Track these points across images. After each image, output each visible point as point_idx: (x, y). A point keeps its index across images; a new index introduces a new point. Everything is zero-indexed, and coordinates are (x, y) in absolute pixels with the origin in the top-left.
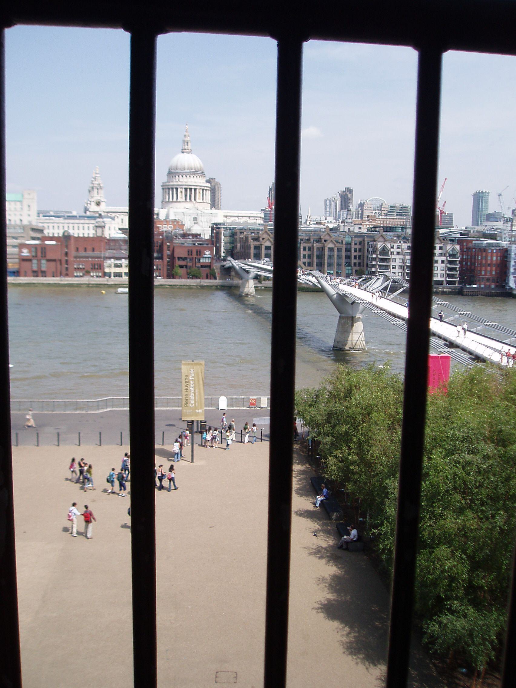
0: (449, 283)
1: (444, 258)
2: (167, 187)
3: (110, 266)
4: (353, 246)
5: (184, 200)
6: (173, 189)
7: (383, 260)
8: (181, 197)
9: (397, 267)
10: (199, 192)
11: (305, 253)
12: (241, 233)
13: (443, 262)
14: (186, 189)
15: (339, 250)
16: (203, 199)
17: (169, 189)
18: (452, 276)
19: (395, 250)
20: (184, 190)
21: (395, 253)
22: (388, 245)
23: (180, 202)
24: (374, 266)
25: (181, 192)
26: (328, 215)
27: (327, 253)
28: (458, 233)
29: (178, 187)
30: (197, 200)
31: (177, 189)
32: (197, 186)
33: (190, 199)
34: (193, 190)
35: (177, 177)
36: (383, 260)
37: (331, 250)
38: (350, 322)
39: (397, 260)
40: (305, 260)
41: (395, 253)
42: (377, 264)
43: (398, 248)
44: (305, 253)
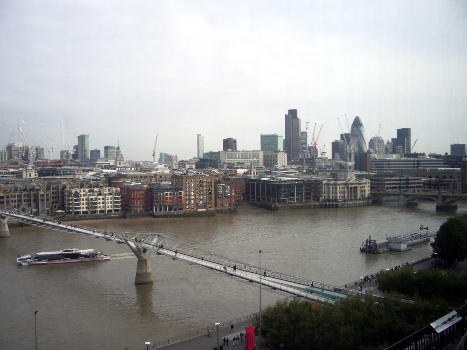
0: (115, 211)
1: (111, 196)
4: (51, 191)
7: (76, 200)
9: (85, 204)
15: (47, 195)
18: (117, 206)
19: (82, 193)
21: (82, 195)
22: (78, 191)
24: (70, 204)
27: (40, 198)
28: (103, 175)
36: (76, 200)
37: (42, 195)
38: (144, 262)
41: (82, 195)
42: (72, 203)
43: (84, 191)
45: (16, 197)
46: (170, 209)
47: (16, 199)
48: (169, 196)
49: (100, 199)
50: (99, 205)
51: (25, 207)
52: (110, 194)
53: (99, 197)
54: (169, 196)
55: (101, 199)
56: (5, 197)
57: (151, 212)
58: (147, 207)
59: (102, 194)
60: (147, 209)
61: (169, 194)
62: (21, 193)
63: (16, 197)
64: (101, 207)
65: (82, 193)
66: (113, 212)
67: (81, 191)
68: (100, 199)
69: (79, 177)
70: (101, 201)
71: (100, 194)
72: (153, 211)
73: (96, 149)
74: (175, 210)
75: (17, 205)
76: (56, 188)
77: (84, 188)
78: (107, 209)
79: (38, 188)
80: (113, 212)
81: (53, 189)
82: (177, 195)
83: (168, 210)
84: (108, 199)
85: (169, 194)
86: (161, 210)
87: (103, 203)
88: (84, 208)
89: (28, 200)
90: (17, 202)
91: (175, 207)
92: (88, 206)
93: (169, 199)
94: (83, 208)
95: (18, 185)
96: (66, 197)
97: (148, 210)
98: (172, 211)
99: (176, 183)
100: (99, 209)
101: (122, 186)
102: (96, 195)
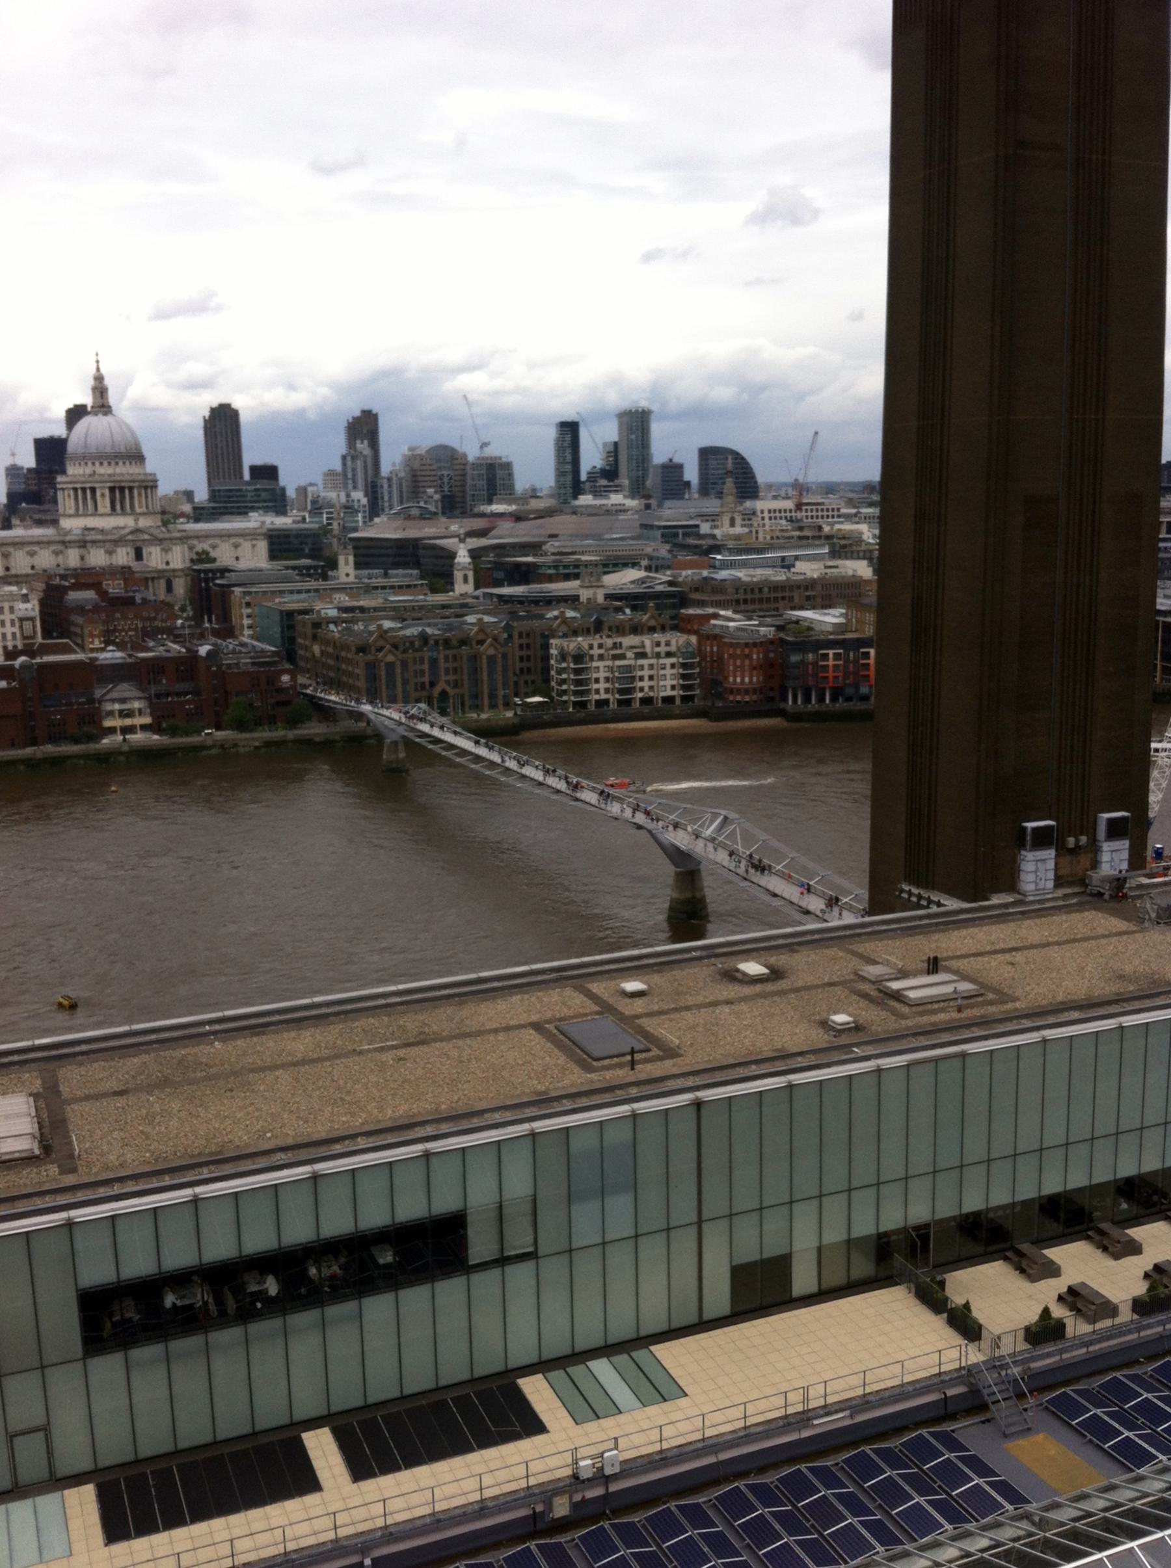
0: (684, 699)
1: (673, 660)
2: (71, 486)
3: (111, 713)
5: (108, 510)
6: (84, 490)
7: (577, 672)
8: (104, 505)
9: (602, 680)
10: (140, 494)
11: (448, 665)
12: (317, 625)
13: (673, 666)
14: (112, 489)
15: (505, 656)
16: (147, 507)
17: (75, 490)
19: (596, 652)
20: (107, 492)
21: (596, 658)
23: (101, 515)
24: (564, 681)
25: (103, 495)
26: (350, 486)
29: (96, 485)
30: (138, 510)
31: (93, 490)
32: (133, 481)
33: (123, 507)
34: (127, 492)
35: (90, 463)
39: (601, 669)
40: (448, 678)
41: (596, 658)
43: (600, 646)
44: (448, 665)
45: (426, 662)
46: (834, 699)
47: (426, 666)
48: (831, 663)
49: (642, 667)
50: (640, 684)
51: (448, 689)
52: (669, 655)
53: (640, 662)
54: (831, 663)
55: (646, 667)
56: (398, 663)
57: (782, 705)
58: (772, 689)
59: (650, 655)
60: (771, 694)
61: (831, 656)
62: (438, 651)
63: (426, 662)
64: (646, 689)
65: (596, 652)
66: (678, 701)
67: (591, 647)
68: (642, 667)
69: (595, 594)
70: (646, 673)
71: (643, 655)
72: (785, 700)
73: (671, 460)
74: (849, 699)
75: (427, 684)
76: (528, 635)
77: (601, 637)
78: (663, 694)
79: (481, 637)
80: (678, 701)
81: (520, 635)
82: (854, 657)
83: (827, 701)
84: (664, 669)
85: (831, 656)
86: (807, 700)
87: (651, 678)
88: (600, 689)
89: (455, 670)
90: (427, 674)
91: (850, 691)
92: (611, 686)
93: (831, 669)
94: (597, 691)
95: (429, 630)
96: (552, 662)
97: (772, 699)
98: (841, 705)
99: (857, 621)
100: (640, 695)
101: (706, 629)
102: (633, 656)
